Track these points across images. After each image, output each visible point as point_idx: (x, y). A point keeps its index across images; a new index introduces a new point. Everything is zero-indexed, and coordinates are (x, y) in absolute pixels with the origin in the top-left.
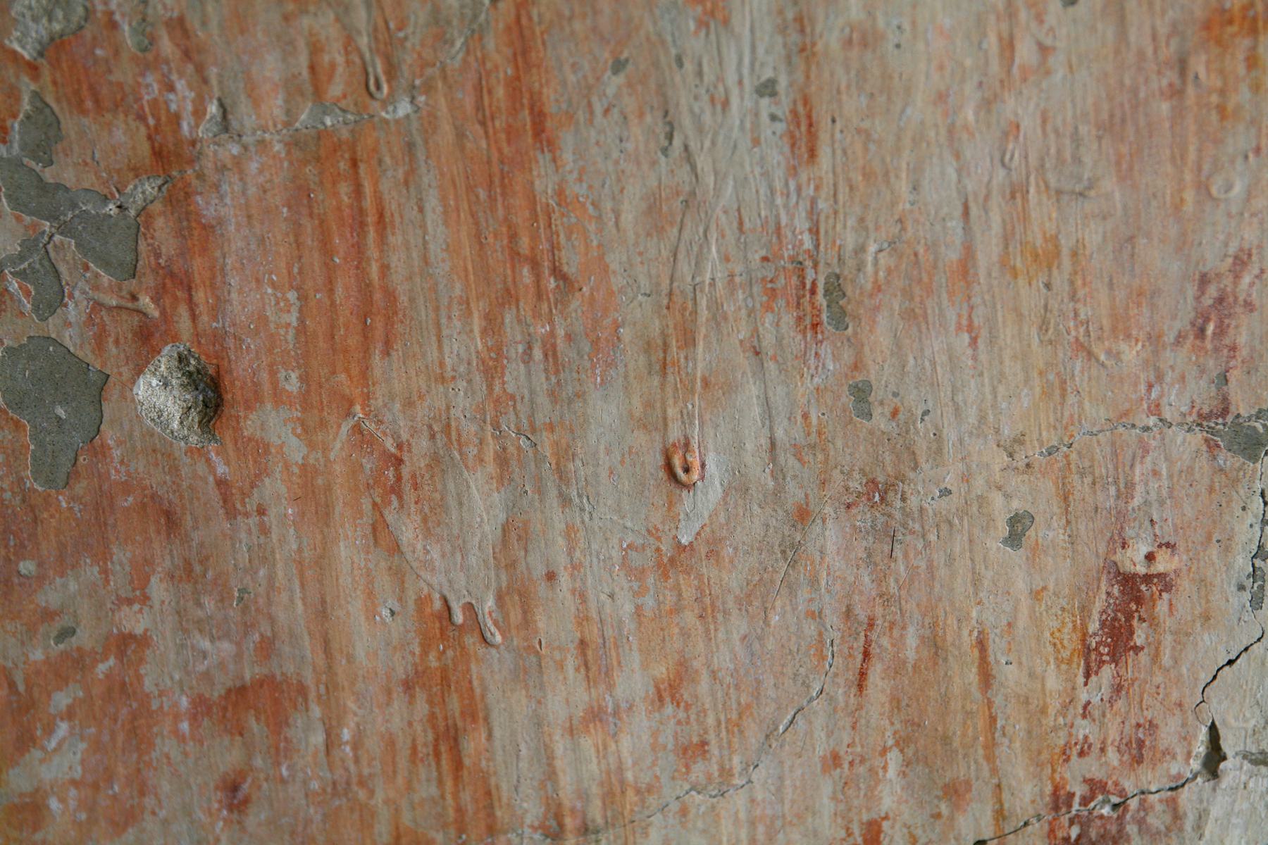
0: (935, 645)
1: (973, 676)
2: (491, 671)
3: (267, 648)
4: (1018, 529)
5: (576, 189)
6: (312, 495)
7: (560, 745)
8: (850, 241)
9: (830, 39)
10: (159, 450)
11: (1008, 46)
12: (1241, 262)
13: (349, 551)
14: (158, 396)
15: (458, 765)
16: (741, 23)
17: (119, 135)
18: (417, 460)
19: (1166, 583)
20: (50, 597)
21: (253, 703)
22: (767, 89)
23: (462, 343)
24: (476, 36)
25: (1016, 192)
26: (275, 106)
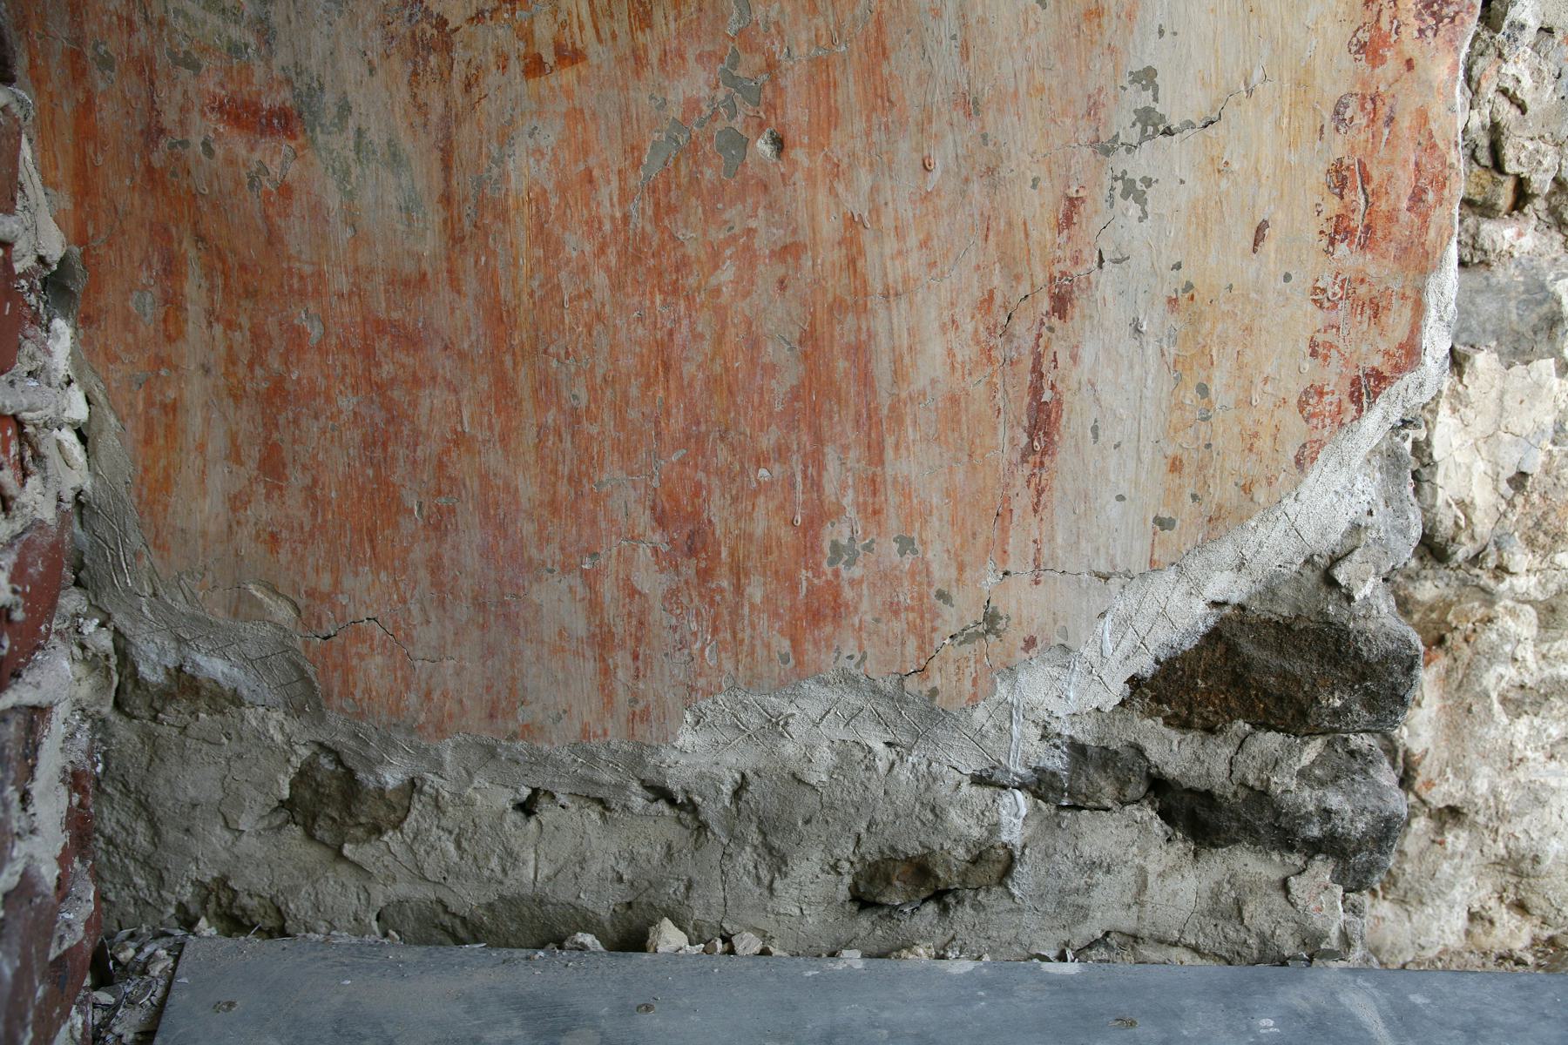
0: (1010, 224)
1: (1022, 235)
2: (867, 237)
3: (795, 231)
4: (1035, 181)
5: (895, 73)
6: (811, 178)
7: (889, 263)
8: (980, 86)
9: (973, 21)
10: (763, 164)
11: (1026, 22)
12: (1100, 90)
13: (822, 197)
14: (763, 147)
15: (855, 271)
16: (946, 17)
17: (757, 59)
18: (844, 166)
19: (1082, 200)
20: (726, 216)
21: (789, 251)
22: (954, 37)
23: (859, 125)
24: (866, 23)
25: (1030, 69)
26: (804, 48)
